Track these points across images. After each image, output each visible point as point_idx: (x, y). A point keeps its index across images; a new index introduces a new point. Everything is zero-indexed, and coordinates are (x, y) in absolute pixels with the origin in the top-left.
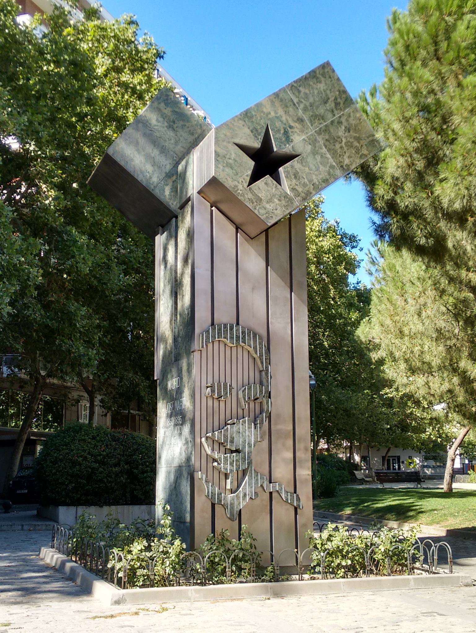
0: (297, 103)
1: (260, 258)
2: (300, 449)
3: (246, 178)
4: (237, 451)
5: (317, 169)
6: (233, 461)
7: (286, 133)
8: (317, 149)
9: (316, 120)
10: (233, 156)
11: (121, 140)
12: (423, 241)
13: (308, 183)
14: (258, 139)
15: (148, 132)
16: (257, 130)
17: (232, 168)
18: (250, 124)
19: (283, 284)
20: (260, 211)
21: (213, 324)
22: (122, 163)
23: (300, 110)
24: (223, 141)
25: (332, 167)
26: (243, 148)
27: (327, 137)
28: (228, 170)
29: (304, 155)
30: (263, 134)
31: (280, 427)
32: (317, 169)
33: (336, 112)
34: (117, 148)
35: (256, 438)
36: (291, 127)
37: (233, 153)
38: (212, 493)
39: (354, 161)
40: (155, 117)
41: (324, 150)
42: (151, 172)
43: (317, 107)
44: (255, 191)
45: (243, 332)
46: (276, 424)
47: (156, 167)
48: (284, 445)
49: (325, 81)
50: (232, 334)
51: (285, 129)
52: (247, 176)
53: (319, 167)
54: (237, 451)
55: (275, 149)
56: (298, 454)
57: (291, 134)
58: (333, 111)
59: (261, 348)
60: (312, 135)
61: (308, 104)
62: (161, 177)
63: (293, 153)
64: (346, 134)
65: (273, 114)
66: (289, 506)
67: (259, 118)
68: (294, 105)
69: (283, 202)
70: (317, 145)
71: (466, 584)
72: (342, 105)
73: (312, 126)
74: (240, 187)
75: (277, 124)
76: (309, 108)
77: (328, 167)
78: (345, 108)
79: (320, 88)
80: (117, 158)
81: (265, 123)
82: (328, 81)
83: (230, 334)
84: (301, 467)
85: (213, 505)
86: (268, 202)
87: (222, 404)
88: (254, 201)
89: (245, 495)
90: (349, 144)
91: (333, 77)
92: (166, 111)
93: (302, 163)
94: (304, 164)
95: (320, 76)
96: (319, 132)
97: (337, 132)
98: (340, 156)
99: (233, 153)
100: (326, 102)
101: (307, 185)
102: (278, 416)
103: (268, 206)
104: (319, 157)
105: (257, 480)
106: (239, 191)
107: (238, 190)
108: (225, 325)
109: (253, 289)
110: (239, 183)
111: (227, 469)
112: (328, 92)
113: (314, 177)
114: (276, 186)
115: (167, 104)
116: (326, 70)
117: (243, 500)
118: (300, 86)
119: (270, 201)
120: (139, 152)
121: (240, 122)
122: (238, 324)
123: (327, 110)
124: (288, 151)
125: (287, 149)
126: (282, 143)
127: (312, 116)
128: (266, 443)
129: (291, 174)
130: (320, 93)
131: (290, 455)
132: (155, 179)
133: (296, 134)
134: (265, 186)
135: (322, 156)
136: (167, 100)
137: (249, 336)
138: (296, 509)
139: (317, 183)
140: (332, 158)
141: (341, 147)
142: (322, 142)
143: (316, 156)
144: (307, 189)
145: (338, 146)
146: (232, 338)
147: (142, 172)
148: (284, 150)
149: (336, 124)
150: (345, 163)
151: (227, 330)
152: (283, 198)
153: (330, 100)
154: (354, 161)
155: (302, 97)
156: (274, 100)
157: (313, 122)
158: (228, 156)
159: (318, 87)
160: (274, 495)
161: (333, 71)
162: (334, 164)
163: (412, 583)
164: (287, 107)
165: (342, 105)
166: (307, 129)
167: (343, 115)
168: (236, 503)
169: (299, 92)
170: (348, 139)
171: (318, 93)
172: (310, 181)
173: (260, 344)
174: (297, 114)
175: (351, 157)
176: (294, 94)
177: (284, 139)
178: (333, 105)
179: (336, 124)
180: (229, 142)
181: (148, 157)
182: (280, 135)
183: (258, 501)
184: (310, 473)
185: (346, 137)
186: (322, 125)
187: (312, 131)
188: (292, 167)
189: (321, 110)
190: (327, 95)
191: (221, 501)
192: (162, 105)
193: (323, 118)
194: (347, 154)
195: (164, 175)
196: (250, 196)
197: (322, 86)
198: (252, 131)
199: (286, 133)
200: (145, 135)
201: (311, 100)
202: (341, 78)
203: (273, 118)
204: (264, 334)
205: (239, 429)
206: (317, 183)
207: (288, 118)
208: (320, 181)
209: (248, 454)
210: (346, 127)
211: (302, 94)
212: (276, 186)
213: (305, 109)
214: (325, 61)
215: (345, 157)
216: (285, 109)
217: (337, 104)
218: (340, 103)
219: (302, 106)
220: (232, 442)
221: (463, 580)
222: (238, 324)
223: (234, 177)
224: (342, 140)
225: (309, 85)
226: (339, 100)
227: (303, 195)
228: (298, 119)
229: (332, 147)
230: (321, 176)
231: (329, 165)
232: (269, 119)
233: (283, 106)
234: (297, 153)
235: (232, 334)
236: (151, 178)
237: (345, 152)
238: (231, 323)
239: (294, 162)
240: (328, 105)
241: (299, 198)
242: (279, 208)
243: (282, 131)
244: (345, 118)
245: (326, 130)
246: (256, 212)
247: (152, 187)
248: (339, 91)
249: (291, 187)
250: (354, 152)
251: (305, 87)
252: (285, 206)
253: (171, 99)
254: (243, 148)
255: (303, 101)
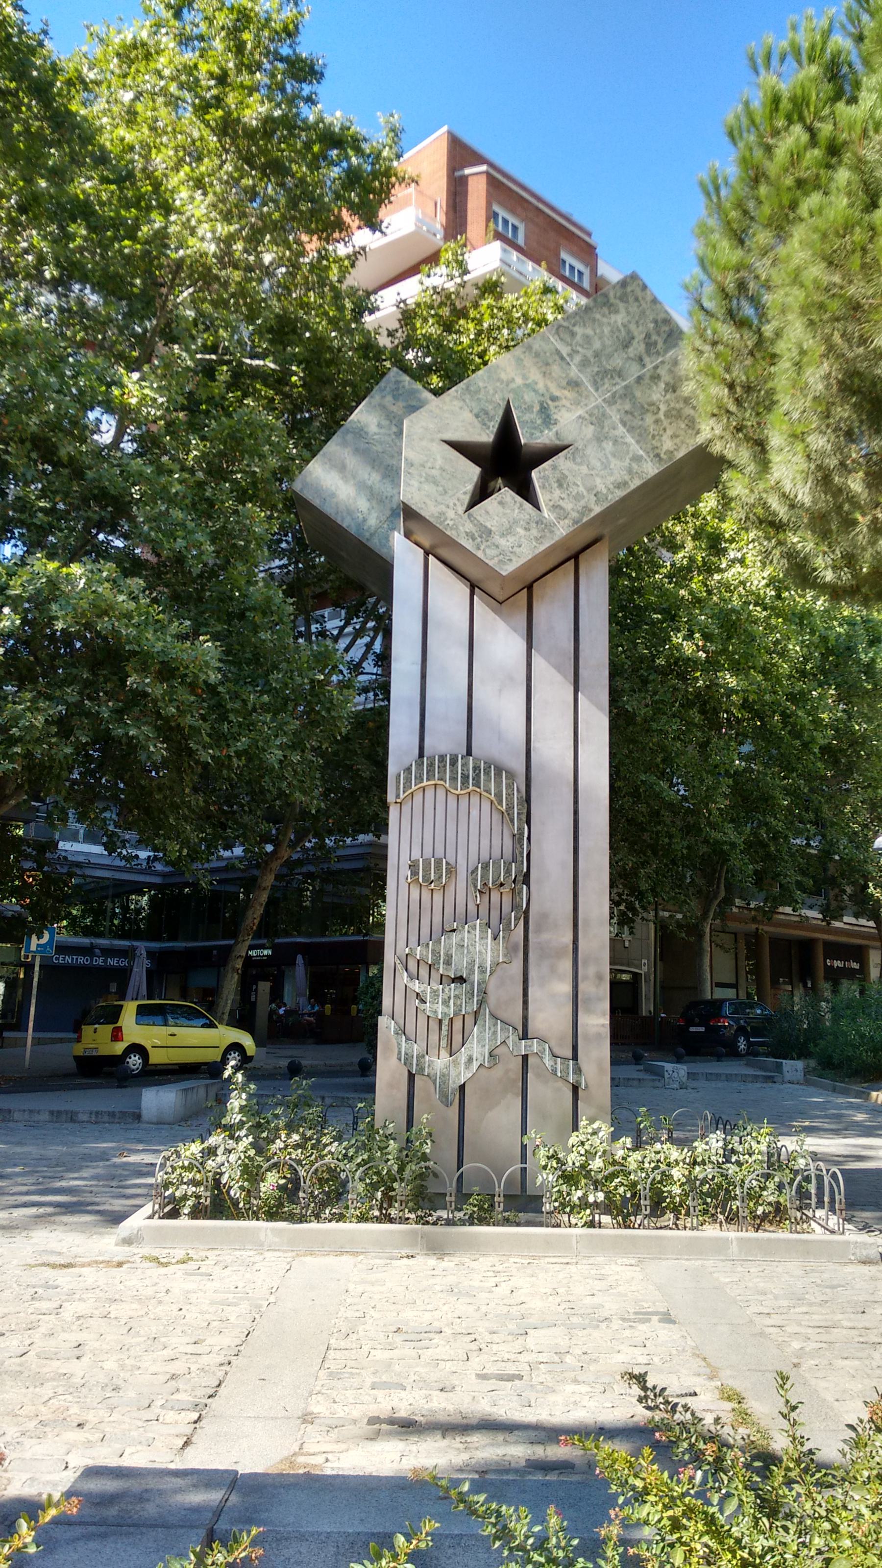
0: (569, 355)
1: (515, 635)
2: (586, 978)
3: (463, 497)
4: (460, 980)
5: (606, 466)
6: (449, 998)
7: (544, 410)
8: (606, 429)
9: (606, 380)
10: (439, 462)
11: (316, 466)
12: (829, 576)
13: (585, 493)
14: (488, 428)
15: (363, 446)
16: (487, 413)
17: (436, 483)
18: (474, 404)
19: (558, 677)
20: (488, 551)
21: (421, 755)
22: (316, 502)
23: (573, 367)
24: (421, 439)
25: (637, 459)
26: (457, 446)
27: (628, 407)
28: (428, 488)
29: (579, 444)
30: (498, 419)
31: (545, 936)
32: (606, 466)
33: (647, 360)
34: (308, 480)
35: (496, 954)
36: (554, 399)
37: (438, 457)
38: (406, 1054)
39: (682, 442)
40: (375, 421)
41: (621, 430)
42: (365, 510)
43: (609, 356)
44: (479, 518)
45: (476, 768)
46: (539, 931)
47: (374, 503)
48: (553, 970)
49: (627, 308)
50: (454, 772)
51: (541, 404)
52: (465, 493)
53: (609, 462)
54: (460, 980)
55: (523, 442)
56: (581, 987)
57: (553, 410)
58: (641, 359)
59: (510, 795)
60: (597, 407)
61: (590, 354)
62: (383, 518)
63: (558, 442)
64: (668, 396)
65: (519, 381)
66: (560, 1084)
67: (491, 392)
68: (562, 358)
69: (534, 532)
70: (607, 423)
71: (864, 1259)
72: (660, 345)
73: (597, 390)
74: (451, 514)
75: (526, 397)
76: (592, 360)
77: (628, 461)
78: (666, 351)
79: (616, 322)
80: (308, 495)
81: (503, 399)
82: (634, 308)
83: (451, 771)
84: (588, 1011)
85: (411, 1077)
86: (503, 535)
87: (438, 897)
88: (476, 535)
89: (470, 1060)
90: (674, 413)
91: (644, 299)
92: (394, 409)
93: (574, 459)
94: (578, 460)
95: (618, 301)
96: (611, 401)
97: (650, 396)
98: (653, 437)
99: (438, 457)
100: (626, 345)
101: (584, 497)
102: (544, 916)
103: (503, 542)
104: (611, 444)
105: (495, 1033)
106: (448, 522)
107: (446, 519)
108: (442, 758)
109: (500, 691)
110: (448, 507)
111: (436, 1012)
112: (633, 327)
113: (598, 481)
114: (521, 505)
115: (396, 397)
116: (629, 289)
117: (467, 1068)
118: (574, 325)
119: (507, 532)
120: (345, 479)
121: (455, 403)
122: (469, 753)
123: (629, 358)
124: (547, 442)
125: (545, 438)
126: (535, 428)
127: (598, 373)
128: (518, 964)
129: (552, 481)
130: (615, 330)
131: (566, 988)
132: (373, 521)
133: (563, 410)
134: (500, 508)
135: (615, 442)
136: (397, 389)
137: (487, 773)
138: (575, 1089)
139: (605, 491)
140: (638, 442)
141: (657, 421)
142: (616, 417)
143: (604, 444)
144: (583, 503)
145: (649, 419)
146: (454, 779)
147: (350, 512)
148: (539, 441)
149: (647, 380)
150: (665, 448)
151: (445, 766)
152: (534, 525)
153: (636, 340)
154: (682, 442)
155: (577, 344)
156: (522, 356)
157: (600, 383)
158: (429, 465)
159: (612, 321)
160: (531, 1060)
161: (645, 287)
162: (641, 452)
163: (734, 1248)
164: (547, 364)
165: (660, 345)
166: (587, 397)
167: (663, 362)
168: (453, 1073)
169: (573, 334)
170: (672, 405)
171: (612, 332)
172: (589, 490)
173: (509, 787)
174: (567, 375)
175: (677, 436)
176: (561, 339)
177: (539, 422)
178: (642, 348)
179: (647, 380)
180: (432, 440)
181: (362, 486)
182: (533, 416)
183: (498, 1072)
184: (607, 1021)
185: (667, 402)
186: (618, 387)
187: (596, 399)
188: (554, 468)
189: (617, 361)
190: (629, 332)
191: (423, 1069)
192: (389, 399)
193: (619, 373)
194: (669, 432)
195: (388, 513)
196: (469, 527)
197: (619, 318)
198: (477, 416)
199: (544, 410)
200: (357, 451)
201: (597, 345)
202: (660, 298)
203: (519, 387)
204: (521, 769)
205: (463, 940)
206: (605, 491)
207: (549, 384)
208: (611, 487)
209: (479, 984)
210: (667, 384)
211: (578, 338)
212: (521, 505)
213: (585, 364)
214: (629, 273)
215: (664, 438)
216: (543, 369)
217: (650, 345)
218: (656, 343)
219: (577, 359)
220: (448, 963)
221: (858, 1251)
222: (469, 753)
223: (439, 499)
224: (659, 409)
225: (594, 320)
226: (654, 337)
227: (575, 515)
228: (569, 383)
229: (637, 422)
230: (612, 479)
231: (631, 455)
232: (513, 391)
233: (540, 364)
234: (566, 443)
235: (454, 772)
236: (365, 520)
237: (665, 430)
238: (454, 752)
239: (559, 460)
240: (631, 350)
241: (566, 521)
242: (524, 542)
243: (537, 408)
244: (667, 367)
245: (627, 394)
246: (480, 554)
247: (367, 535)
248: (656, 322)
249: (551, 503)
250: (683, 426)
251: (585, 325)
252: (536, 539)
253: (404, 387)
254: (457, 446)
255: (580, 349)
